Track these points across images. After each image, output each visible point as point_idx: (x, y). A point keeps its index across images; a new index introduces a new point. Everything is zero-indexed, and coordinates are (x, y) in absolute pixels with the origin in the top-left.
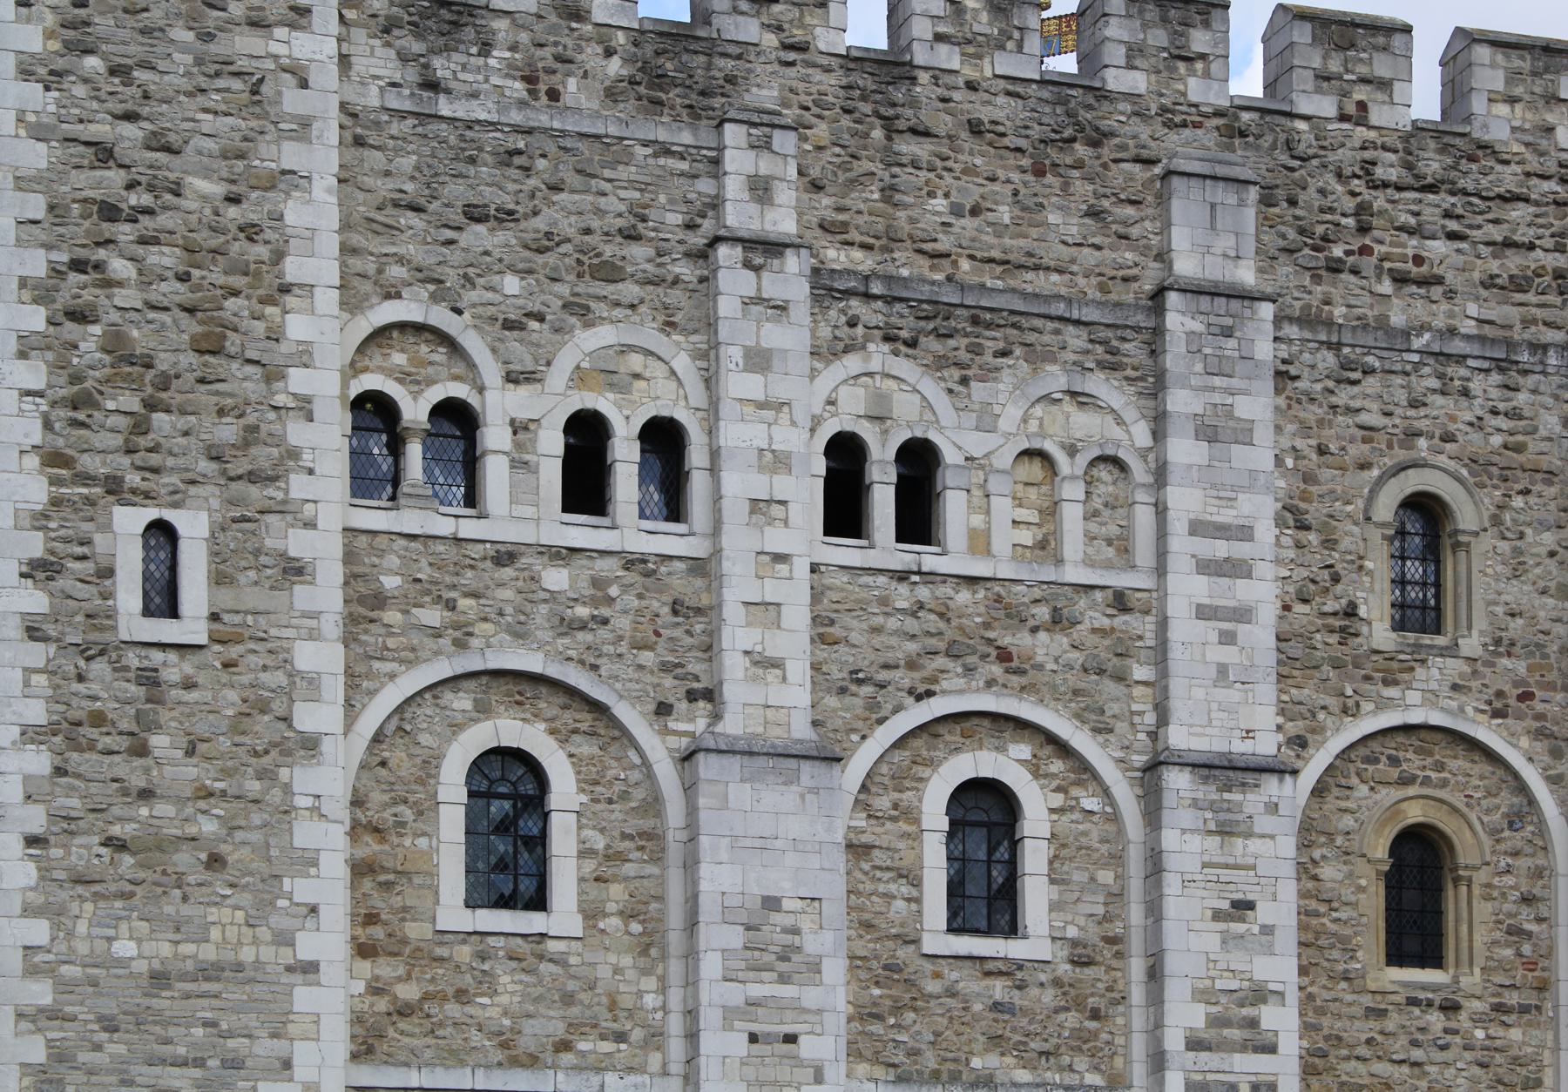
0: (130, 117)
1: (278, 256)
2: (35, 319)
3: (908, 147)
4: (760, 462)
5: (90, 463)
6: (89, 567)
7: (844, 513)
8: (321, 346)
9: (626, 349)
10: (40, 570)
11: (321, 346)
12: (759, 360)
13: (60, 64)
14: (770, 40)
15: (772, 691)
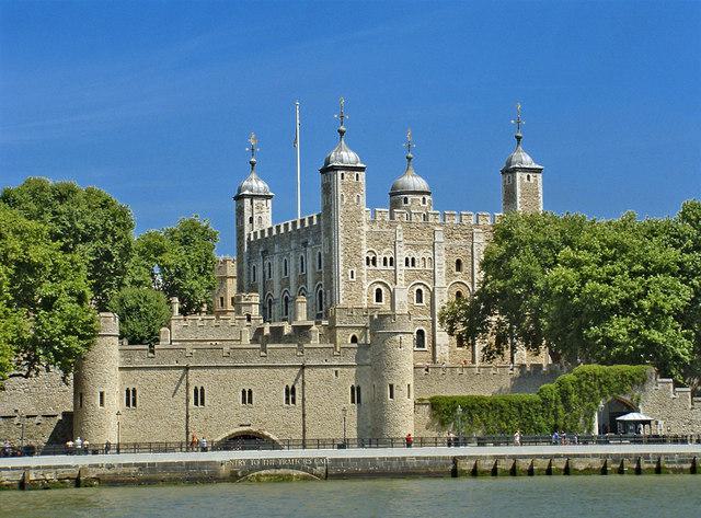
4: (400, 261)
7: (407, 264)
8: (364, 254)
11: (364, 254)
15: (401, 282)
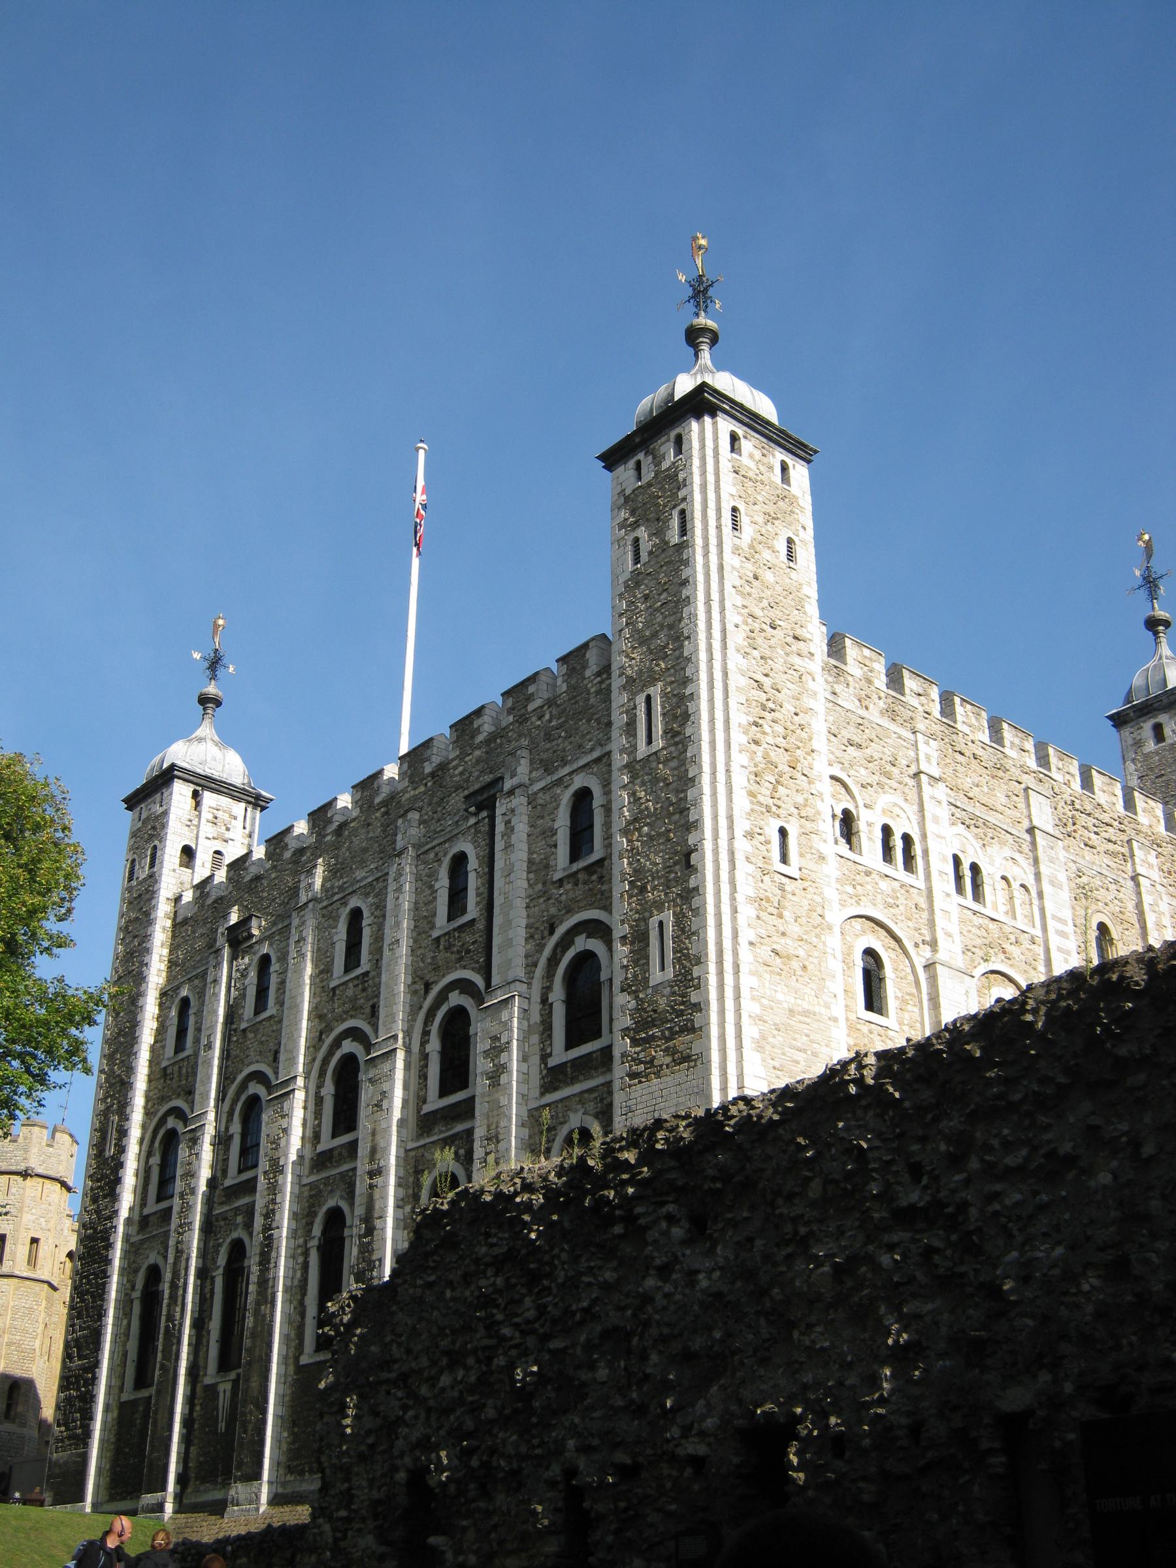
0: (766, 675)
1: (810, 739)
2: (744, 739)
3: (958, 756)
5: (761, 798)
6: (762, 838)
9: (895, 805)
10: (749, 835)
12: (936, 820)
13: (747, 650)
14: (921, 709)
